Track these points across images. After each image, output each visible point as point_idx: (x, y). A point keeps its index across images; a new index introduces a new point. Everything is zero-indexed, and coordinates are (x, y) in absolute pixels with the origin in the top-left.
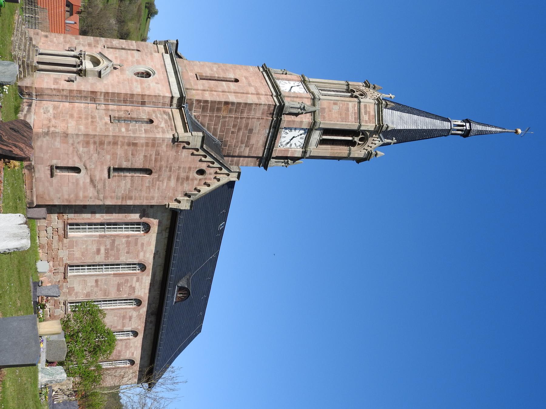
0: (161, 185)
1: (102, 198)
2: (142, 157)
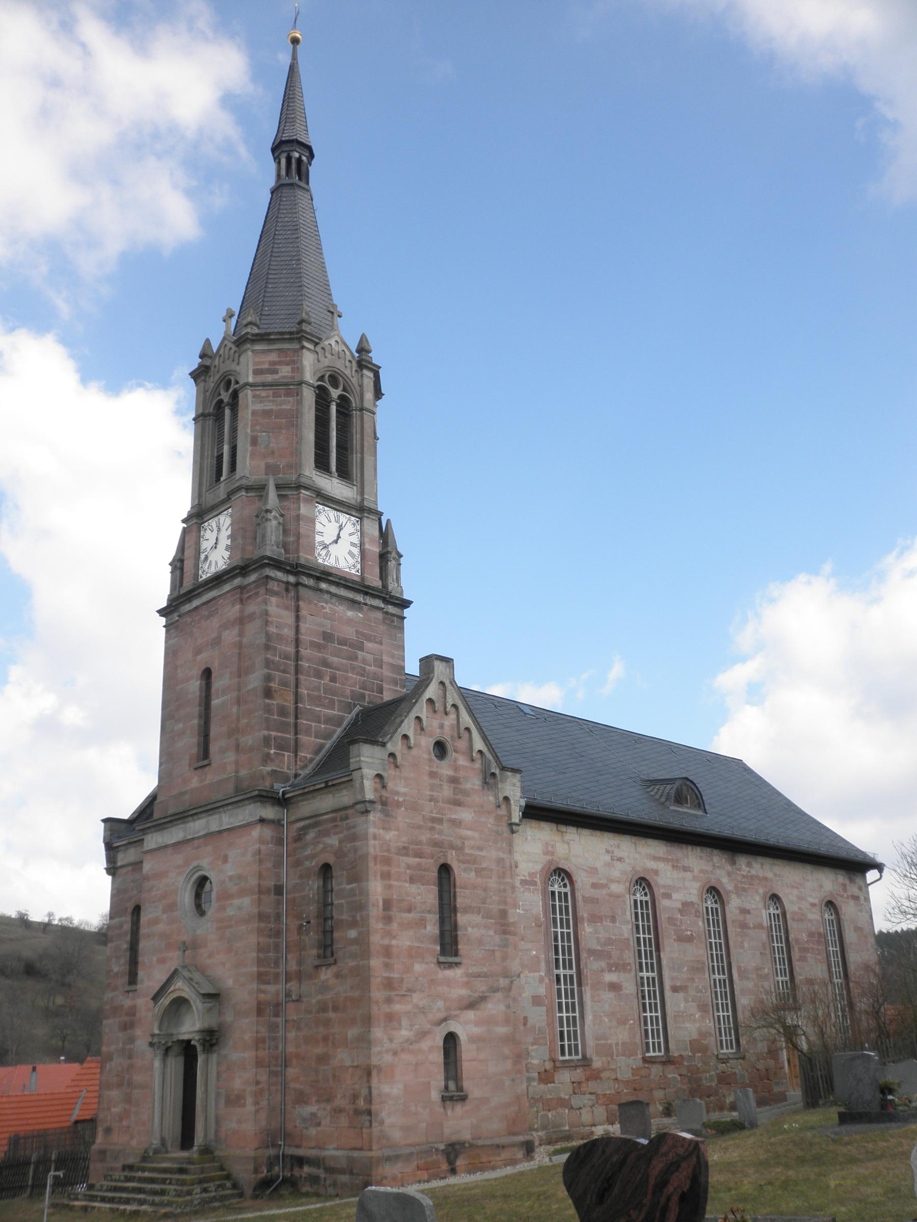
0: (472, 842)
1: (507, 981)
2: (413, 889)
